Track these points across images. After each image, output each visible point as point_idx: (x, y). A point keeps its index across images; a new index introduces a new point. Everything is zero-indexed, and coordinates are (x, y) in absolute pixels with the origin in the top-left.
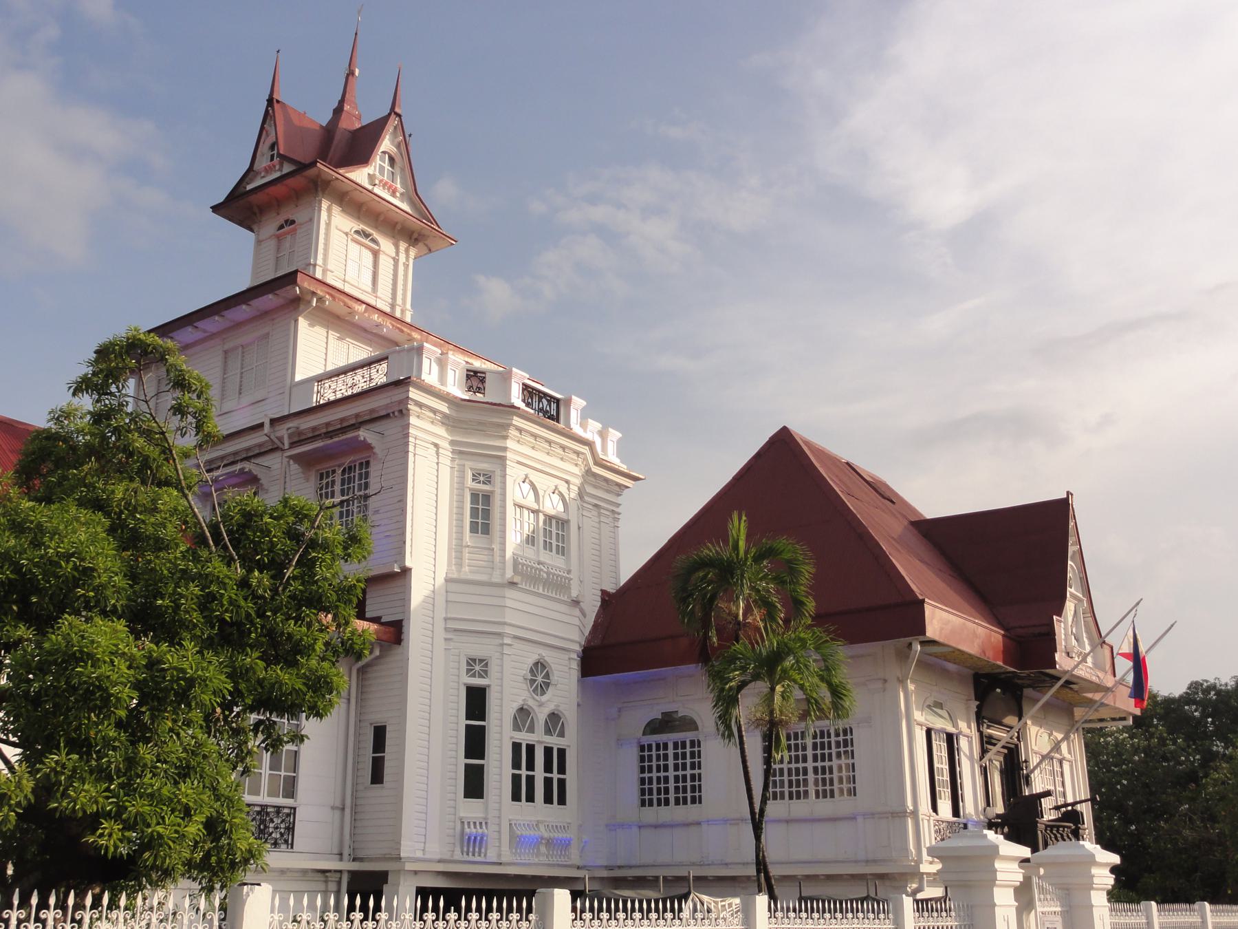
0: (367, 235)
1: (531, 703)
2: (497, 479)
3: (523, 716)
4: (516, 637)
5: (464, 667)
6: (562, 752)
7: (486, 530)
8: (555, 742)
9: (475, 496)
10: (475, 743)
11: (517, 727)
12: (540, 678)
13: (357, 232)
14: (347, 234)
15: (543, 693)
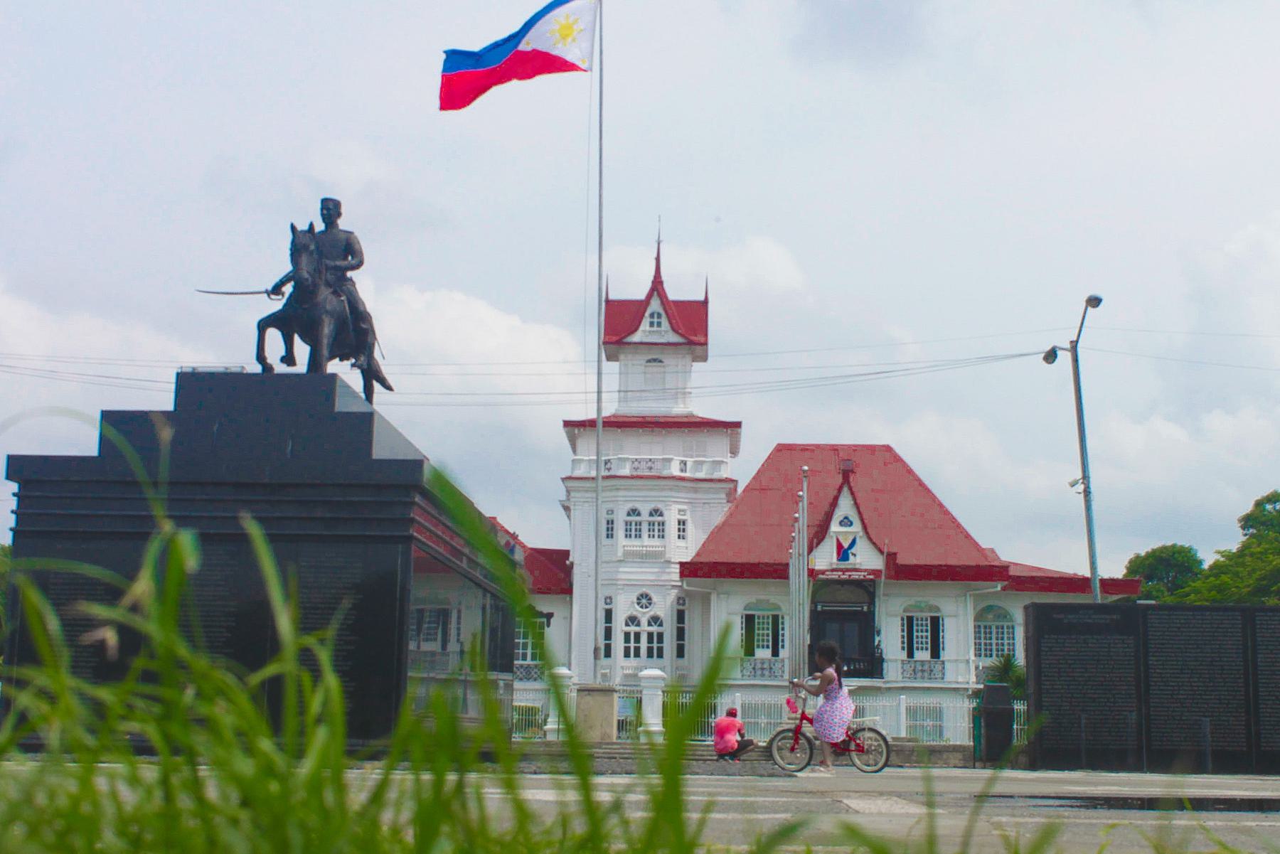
0: (655, 360)
1: (635, 613)
2: (615, 513)
3: (632, 620)
4: (624, 585)
5: (604, 600)
6: (660, 636)
7: (612, 537)
8: (654, 629)
9: (608, 524)
10: (608, 634)
11: (627, 625)
12: (644, 599)
13: (649, 361)
14: (641, 365)
15: (647, 607)
